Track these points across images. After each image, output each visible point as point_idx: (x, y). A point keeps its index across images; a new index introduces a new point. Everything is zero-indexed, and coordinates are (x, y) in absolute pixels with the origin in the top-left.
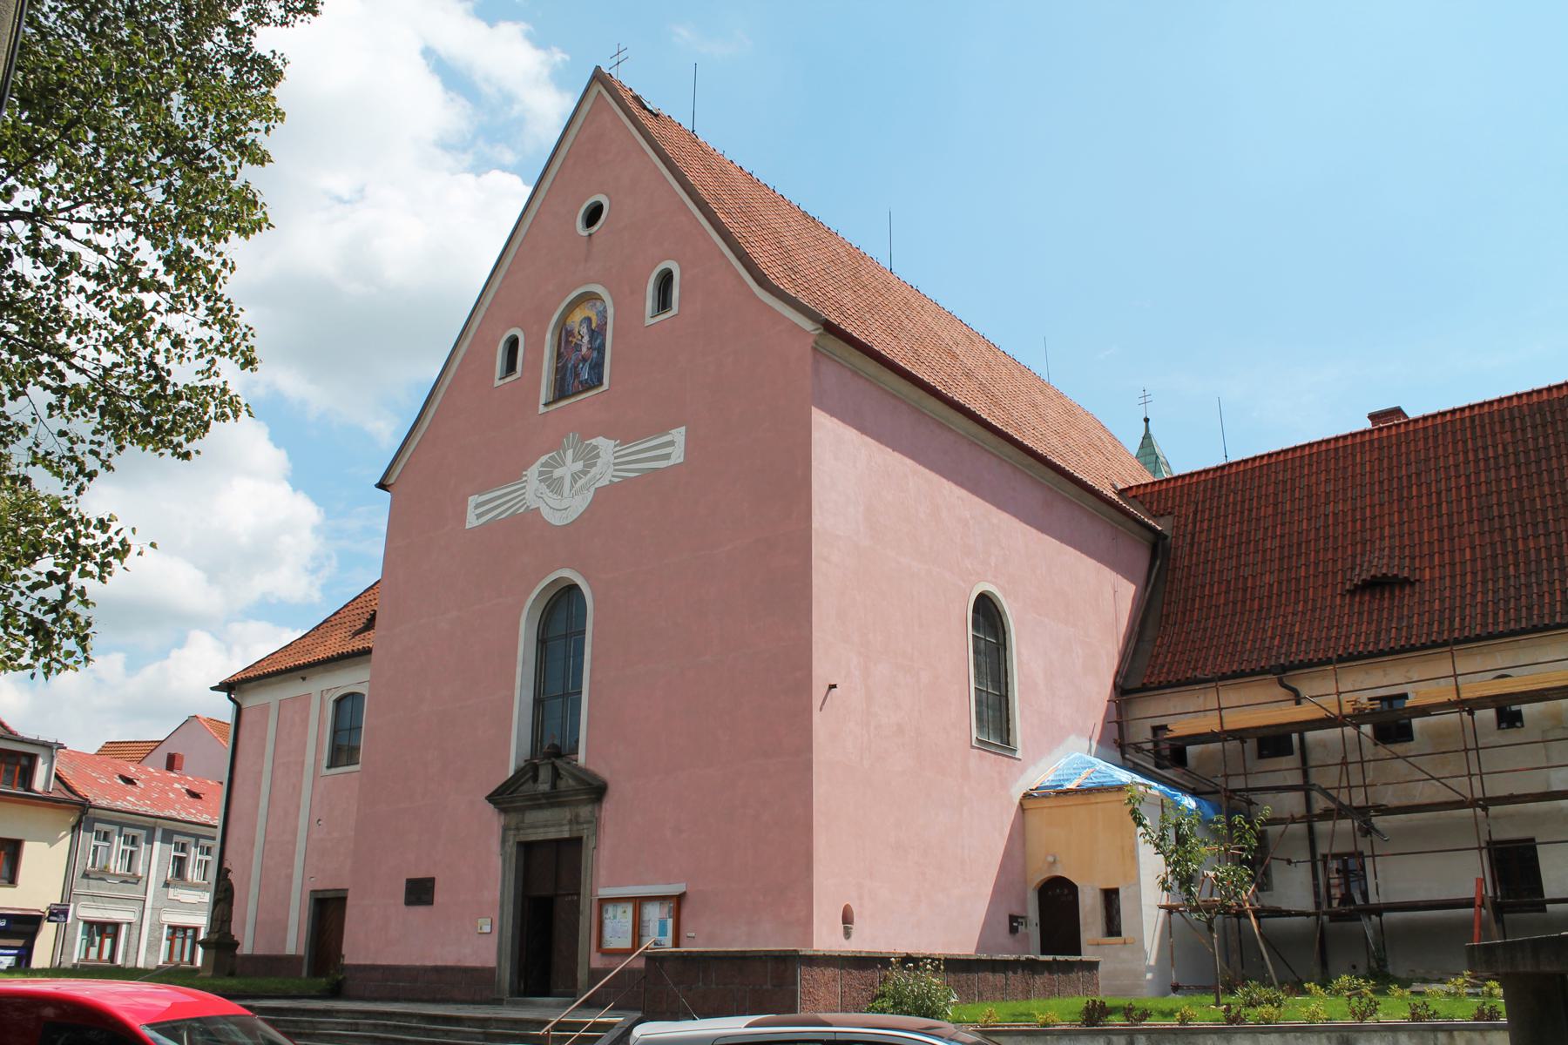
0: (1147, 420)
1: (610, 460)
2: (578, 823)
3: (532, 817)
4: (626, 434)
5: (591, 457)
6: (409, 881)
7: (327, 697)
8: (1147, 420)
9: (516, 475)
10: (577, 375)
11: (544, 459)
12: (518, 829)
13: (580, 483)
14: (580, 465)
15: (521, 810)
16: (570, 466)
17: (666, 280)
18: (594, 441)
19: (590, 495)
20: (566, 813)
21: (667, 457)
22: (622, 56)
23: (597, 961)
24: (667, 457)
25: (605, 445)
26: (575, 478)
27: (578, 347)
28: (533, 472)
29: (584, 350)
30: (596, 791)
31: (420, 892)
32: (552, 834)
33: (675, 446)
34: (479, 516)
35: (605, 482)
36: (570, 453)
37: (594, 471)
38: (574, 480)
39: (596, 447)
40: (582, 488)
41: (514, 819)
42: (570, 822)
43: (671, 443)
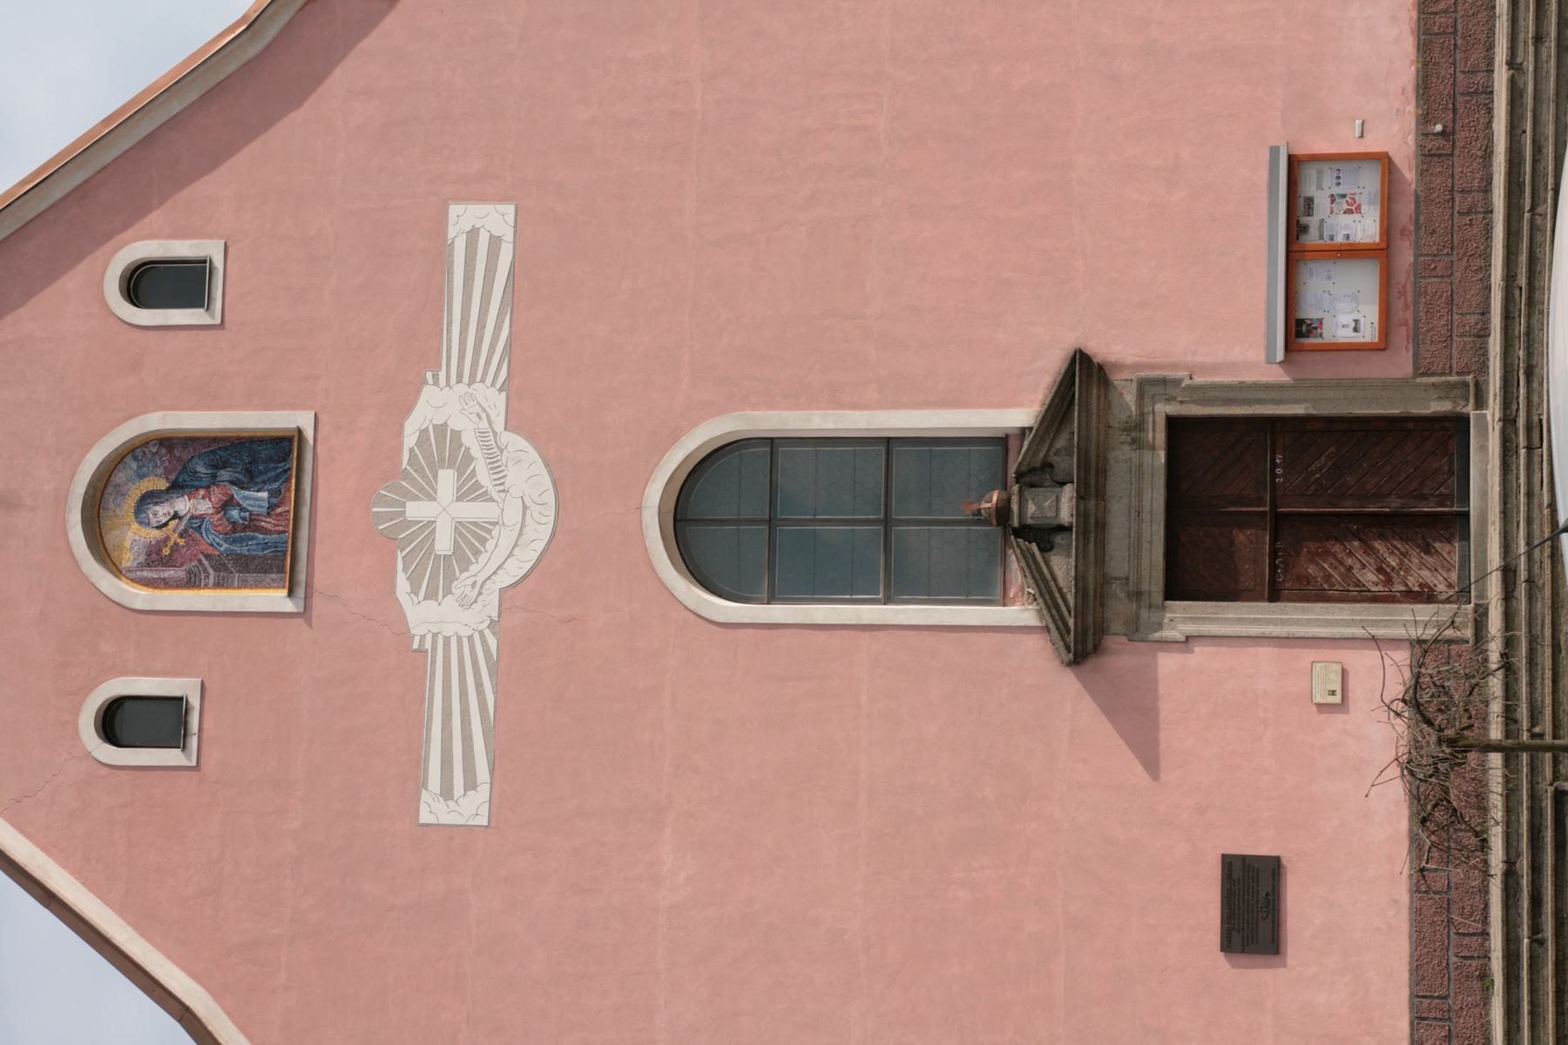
1: (458, 403)
2: (1139, 425)
3: (1118, 561)
4: (419, 355)
5: (445, 447)
6: (1227, 945)
10: (252, 524)
11: (402, 584)
12: (1137, 595)
13: (484, 476)
14: (447, 480)
15: (1105, 581)
16: (439, 510)
17: (143, 284)
18: (410, 440)
19: (516, 443)
20: (1121, 454)
23: (1400, 364)
26: (469, 491)
27: (196, 523)
28: (423, 617)
29: (204, 507)
30: (1083, 376)
31: (1252, 907)
32: (1155, 498)
33: (482, 223)
34: (471, 784)
35: (496, 402)
36: (416, 510)
37: (469, 440)
38: (469, 491)
39: (424, 433)
40: (495, 467)
41: (1119, 608)
42: (1138, 444)
43: (473, 234)
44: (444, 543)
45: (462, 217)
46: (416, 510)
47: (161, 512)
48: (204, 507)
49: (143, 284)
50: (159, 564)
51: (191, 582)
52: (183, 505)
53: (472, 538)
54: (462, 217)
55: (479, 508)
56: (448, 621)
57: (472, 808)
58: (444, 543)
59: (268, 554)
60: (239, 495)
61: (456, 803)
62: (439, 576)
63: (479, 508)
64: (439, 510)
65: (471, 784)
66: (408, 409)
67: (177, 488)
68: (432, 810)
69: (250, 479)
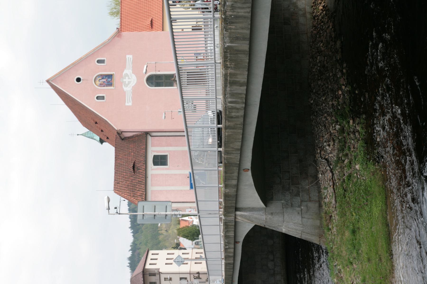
0: (78, 135)
1: (128, 71)
4: (124, 67)
5: (127, 75)
7: (152, 168)
8: (78, 135)
9: (124, 93)
10: (109, 82)
11: (123, 86)
14: (127, 78)
16: (126, 80)
17: (99, 61)
18: (124, 74)
19: (133, 75)
21: (131, 58)
22: (42, 83)
24: (131, 58)
25: (126, 72)
26: (129, 78)
27: (104, 82)
28: (125, 89)
33: (129, 57)
34: (130, 102)
35: (131, 71)
36: (124, 80)
37: (129, 74)
44: (127, 83)
45: (128, 56)
46: (124, 80)
47: (101, 81)
48: (105, 80)
49: (99, 61)
50: (101, 85)
51: (104, 86)
52: (103, 80)
53: (129, 83)
54: (128, 56)
55: (130, 80)
56: (128, 89)
57: (130, 104)
58: (127, 83)
59: (110, 84)
60: (108, 80)
61: (129, 103)
62: (127, 85)
63: (130, 80)
64: (126, 80)
65: (130, 102)
66: (123, 72)
67: (102, 79)
68: (127, 104)
69: (109, 78)
